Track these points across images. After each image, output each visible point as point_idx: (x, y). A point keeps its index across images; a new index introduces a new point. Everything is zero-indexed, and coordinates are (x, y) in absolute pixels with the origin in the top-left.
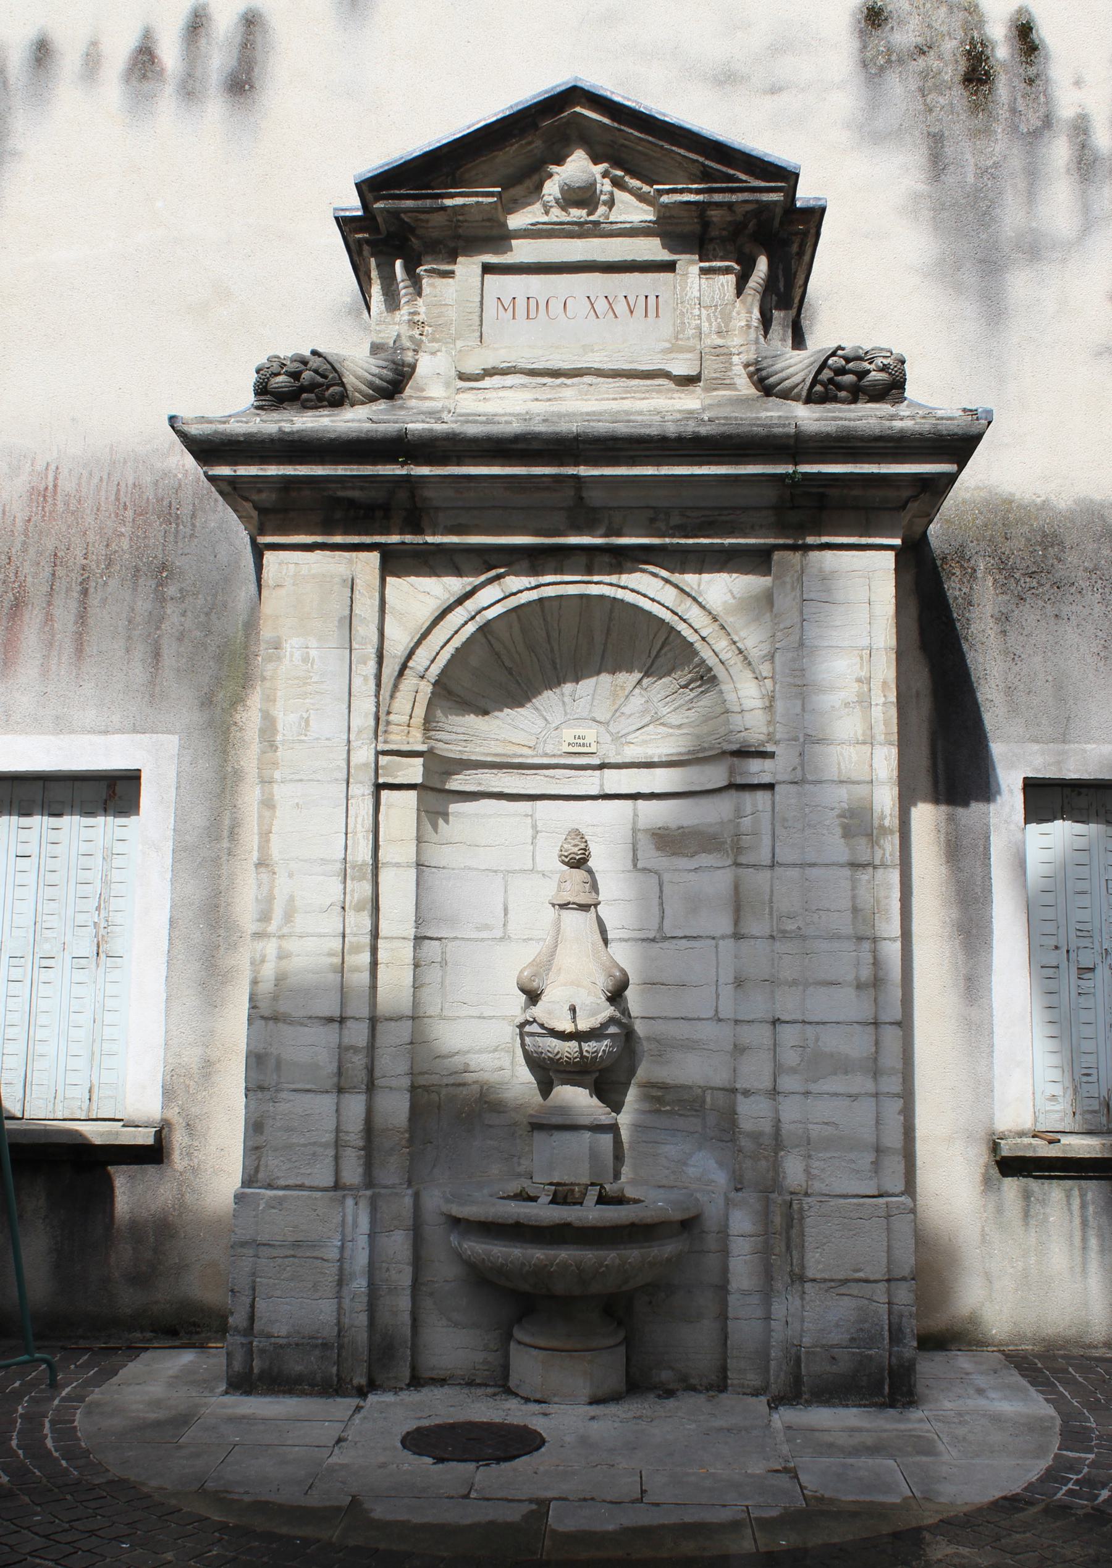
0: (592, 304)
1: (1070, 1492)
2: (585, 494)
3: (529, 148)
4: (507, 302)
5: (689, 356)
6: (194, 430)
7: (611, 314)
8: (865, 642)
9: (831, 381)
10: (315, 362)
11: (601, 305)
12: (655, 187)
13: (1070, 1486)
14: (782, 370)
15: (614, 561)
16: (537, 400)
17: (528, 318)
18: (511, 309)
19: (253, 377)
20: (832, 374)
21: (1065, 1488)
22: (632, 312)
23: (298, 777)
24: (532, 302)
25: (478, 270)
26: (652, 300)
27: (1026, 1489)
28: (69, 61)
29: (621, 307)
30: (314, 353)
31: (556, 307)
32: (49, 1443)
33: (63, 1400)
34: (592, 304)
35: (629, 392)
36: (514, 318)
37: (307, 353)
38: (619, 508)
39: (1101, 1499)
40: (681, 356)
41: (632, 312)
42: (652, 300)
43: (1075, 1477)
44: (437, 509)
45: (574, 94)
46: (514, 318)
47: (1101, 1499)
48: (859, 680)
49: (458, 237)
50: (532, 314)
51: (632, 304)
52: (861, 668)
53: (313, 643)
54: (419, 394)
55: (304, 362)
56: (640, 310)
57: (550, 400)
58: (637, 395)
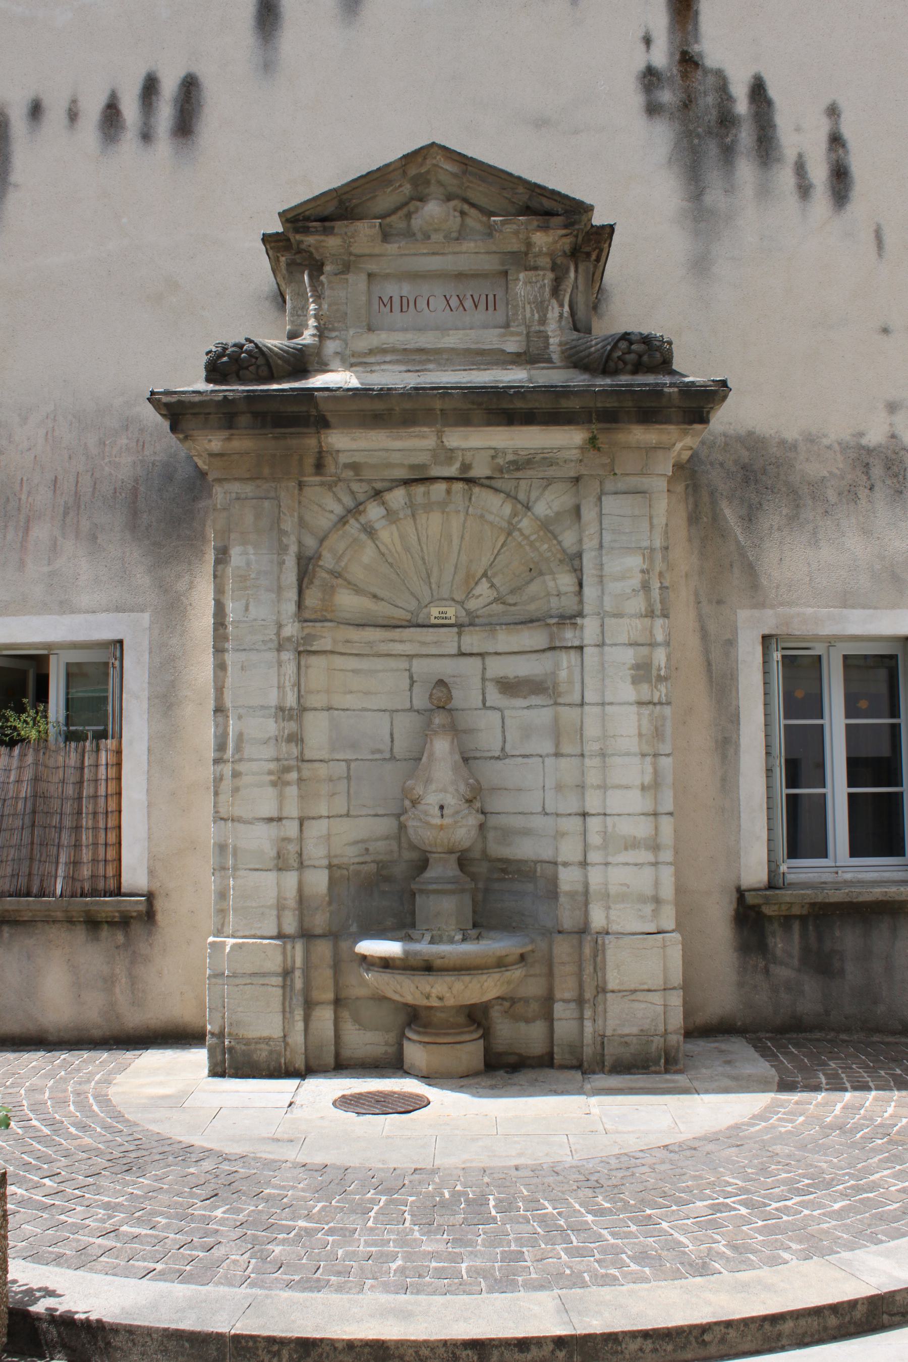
0: (448, 302)
1: (780, 1119)
2: (444, 440)
3: (401, 189)
4: (386, 300)
5: (518, 338)
6: (165, 399)
7: (461, 308)
8: (646, 544)
9: (619, 358)
10: (248, 346)
11: (454, 302)
12: (493, 218)
13: (779, 1115)
14: (585, 350)
15: (466, 487)
16: (409, 371)
17: (402, 311)
18: (389, 305)
19: (205, 359)
20: (620, 353)
21: (775, 1117)
22: (476, 307)
23: (242, 648)
24: (405, 301)
25: (363, 277)
26: (491, 298)
27: (750, 1118)
28: (55, 115)
29: (468, 303)
30: (249, 340)
31: (422, 304)
32: (95, 1108)
33: (97, 1083)
34: (448, 302)
35: (473, 364)
36: (391, 311)
37: (243, 341)
38: (470, 449)
39: (798, 1122)
40: (513, 339)
41: (476, 307)
42: (491, 298)
43: (783, 1110)
44: (338, 451)
45: (433, 144)
46: (391, 311)
47: (798, 1122)
48: (643, 571)
49: (351, 254)
50: (405, 309)
51: (476, 300)
52: (644, 562)
53: (251, 551)
54: (324, 367)
55: (241, 346)
56: (482, 306)
57: (418, 371)
58: (482, 367)
